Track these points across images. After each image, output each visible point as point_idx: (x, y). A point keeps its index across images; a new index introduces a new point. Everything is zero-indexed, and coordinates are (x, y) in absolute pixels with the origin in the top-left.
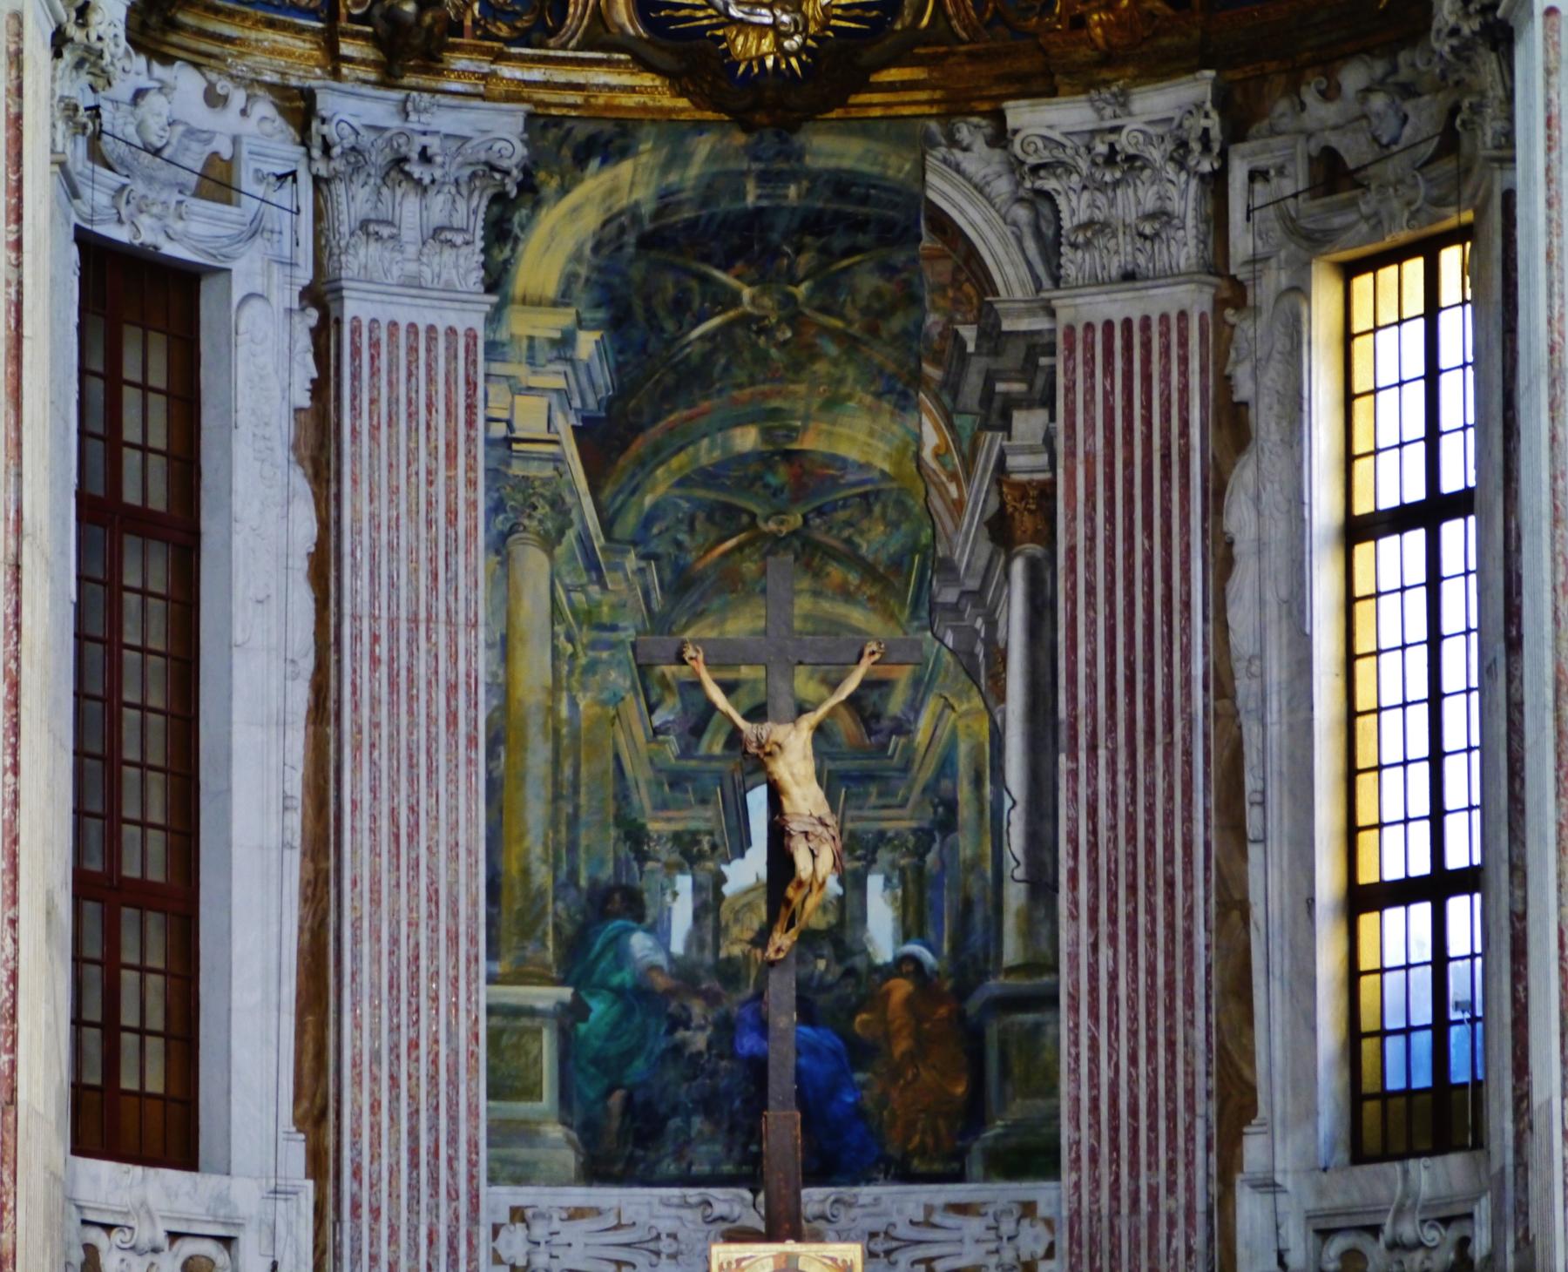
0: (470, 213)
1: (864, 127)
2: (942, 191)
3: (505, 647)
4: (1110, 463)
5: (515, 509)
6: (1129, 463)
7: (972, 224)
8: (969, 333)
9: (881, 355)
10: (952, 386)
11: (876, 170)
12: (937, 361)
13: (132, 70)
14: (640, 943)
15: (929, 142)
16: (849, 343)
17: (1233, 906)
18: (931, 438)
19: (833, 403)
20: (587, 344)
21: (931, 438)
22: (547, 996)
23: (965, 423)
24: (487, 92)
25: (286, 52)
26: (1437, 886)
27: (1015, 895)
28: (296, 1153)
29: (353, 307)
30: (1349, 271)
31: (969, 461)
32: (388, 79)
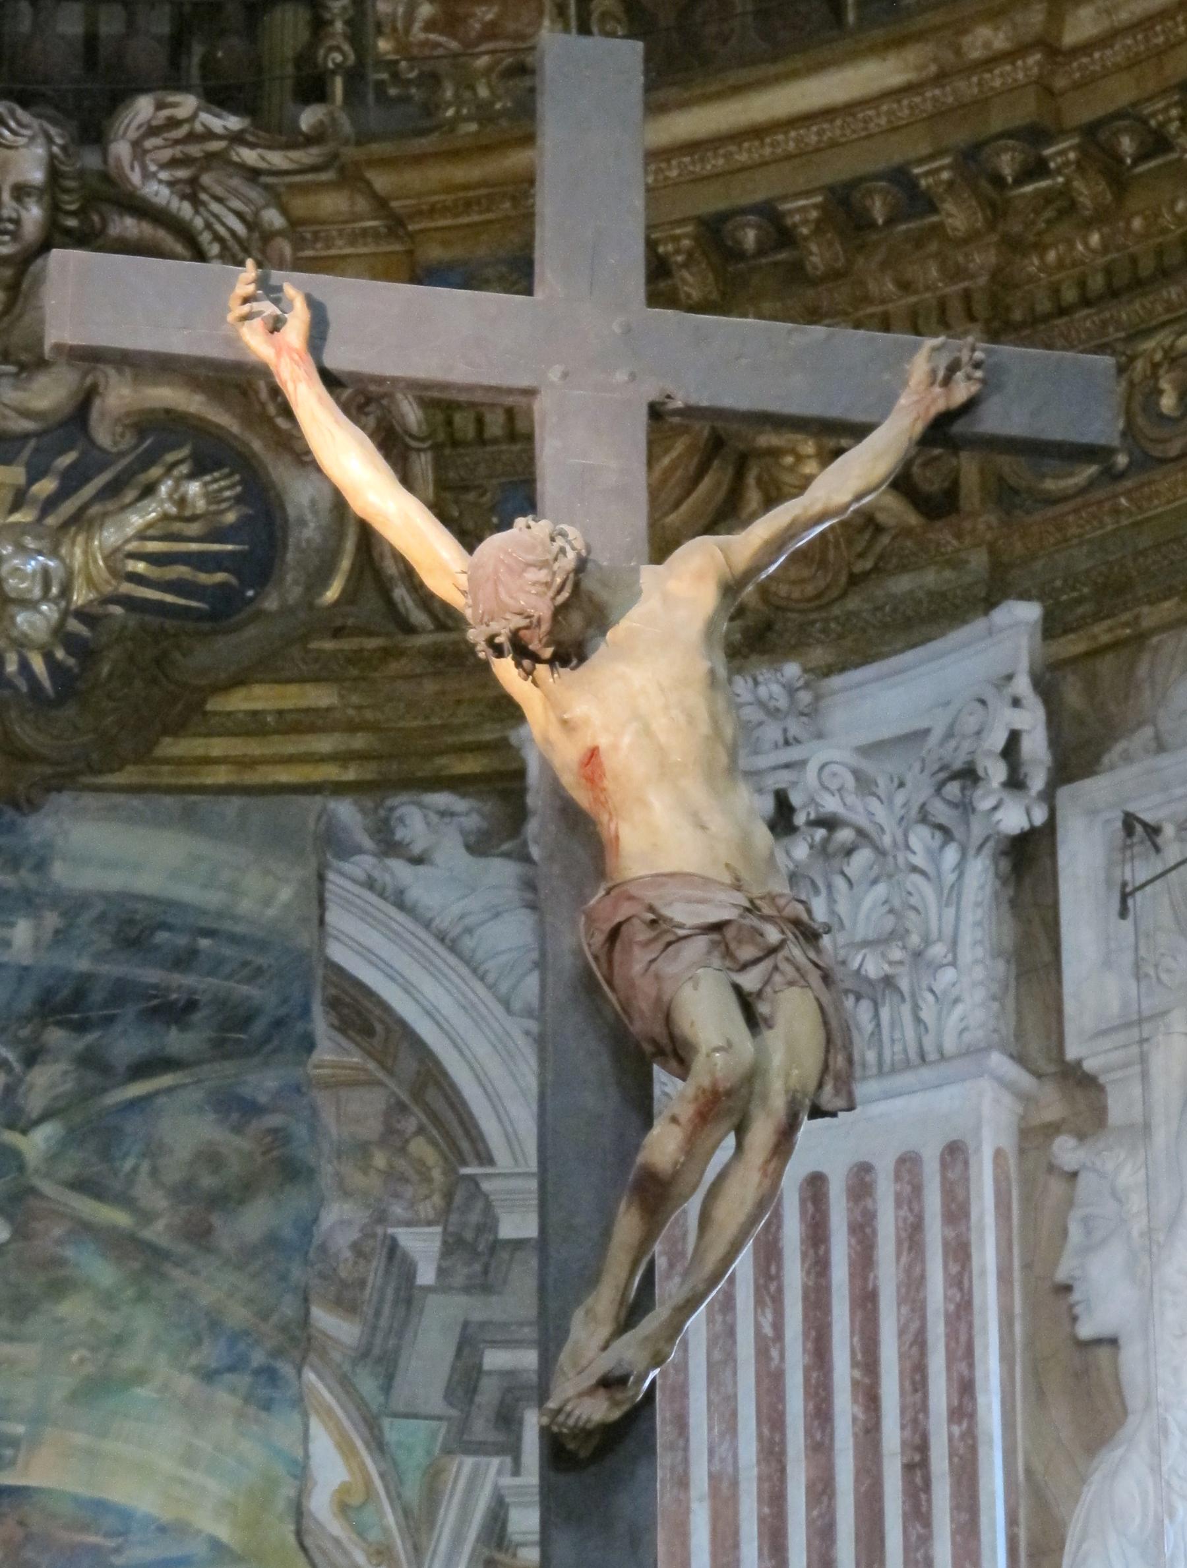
1: (186, 800)
4: (775, 1498)
6: (822, 1489)
7: (430, 1014)
8: (422, 1246)
9: (215, 1287)
10: (385, 1362)
11: (213, 899)
12: (346, 1304)
15: (333, 843)
16: (146, 1260)
18: (330, 1470)
19: (98, 1388)
21: (330, 1470)
23: (413, 1439)
31: (419, 1521)
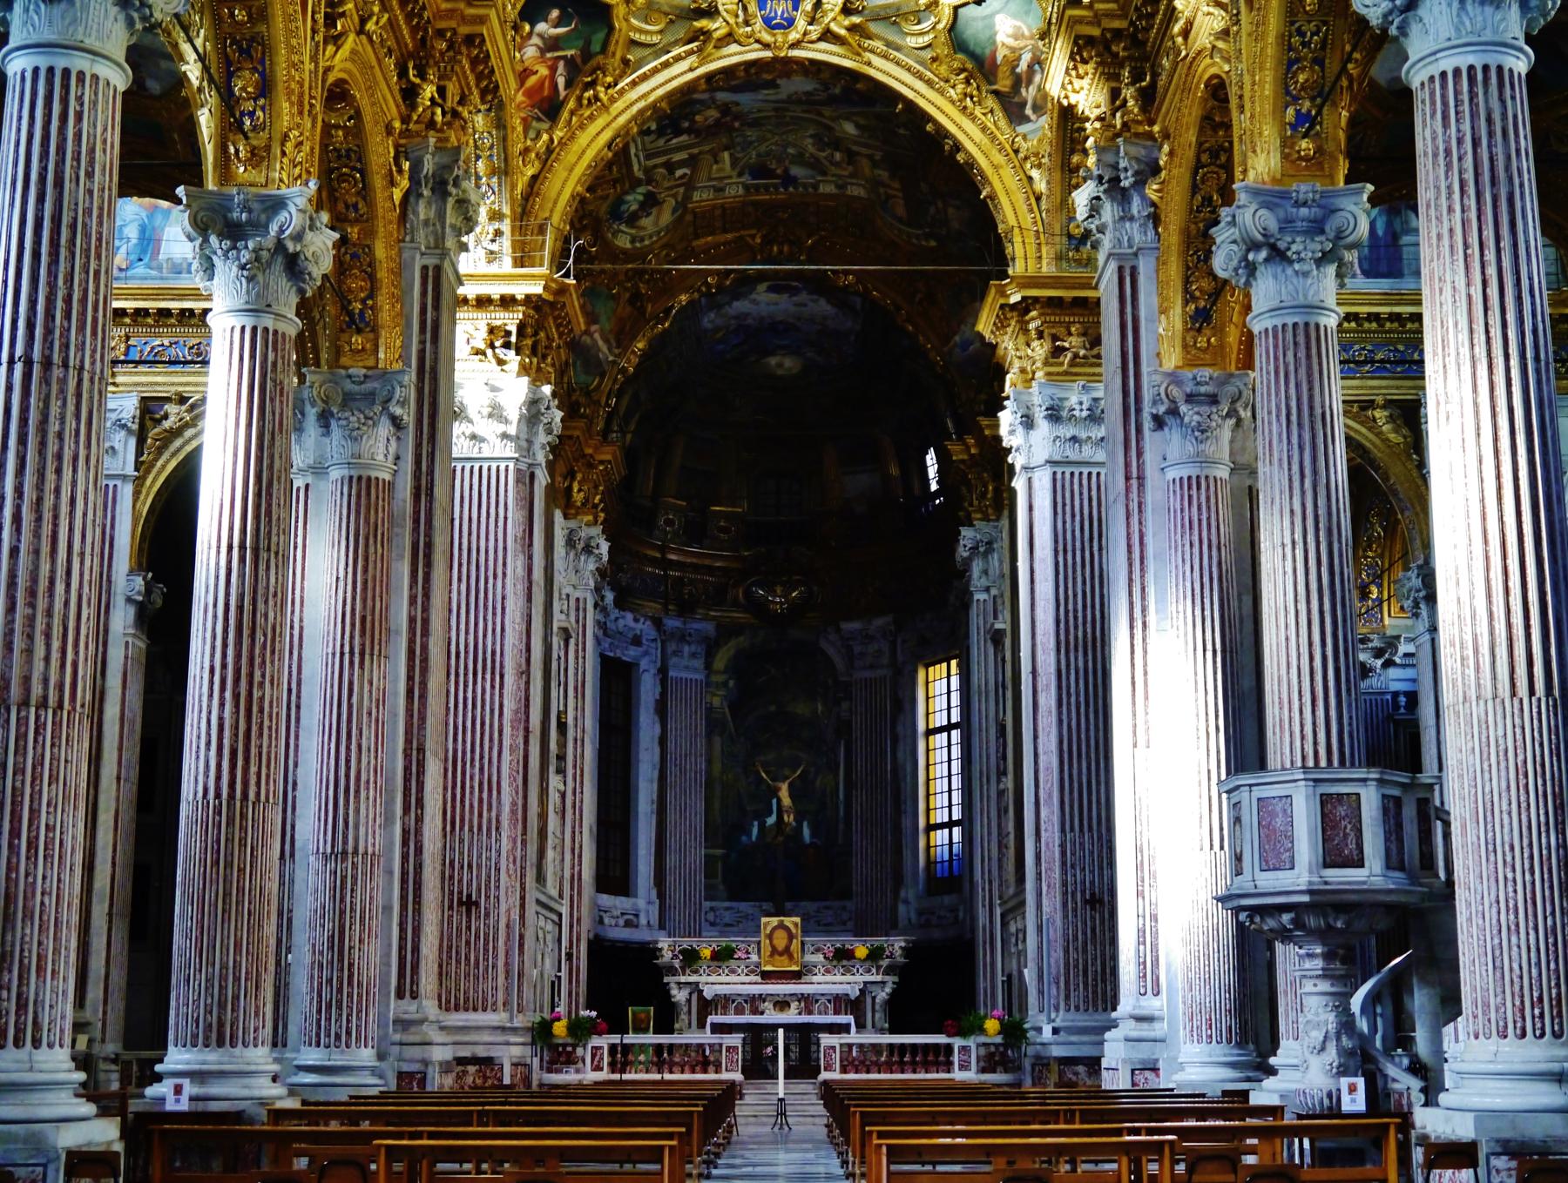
0: (700, 649)
2: (824, 645)
3: (709, 762)
5: (713, 725)
13: (615, 613)
14: (744, 838)
17: (897, 829)
20: (731, 683)
22: (719, 852)
24: (706, 618)
25: (653, 607)
26: (950, 824)
27: (841, 826)
28: (654, 893)
29: (671, 673)
30: (927, 667)
32: (679, 616)
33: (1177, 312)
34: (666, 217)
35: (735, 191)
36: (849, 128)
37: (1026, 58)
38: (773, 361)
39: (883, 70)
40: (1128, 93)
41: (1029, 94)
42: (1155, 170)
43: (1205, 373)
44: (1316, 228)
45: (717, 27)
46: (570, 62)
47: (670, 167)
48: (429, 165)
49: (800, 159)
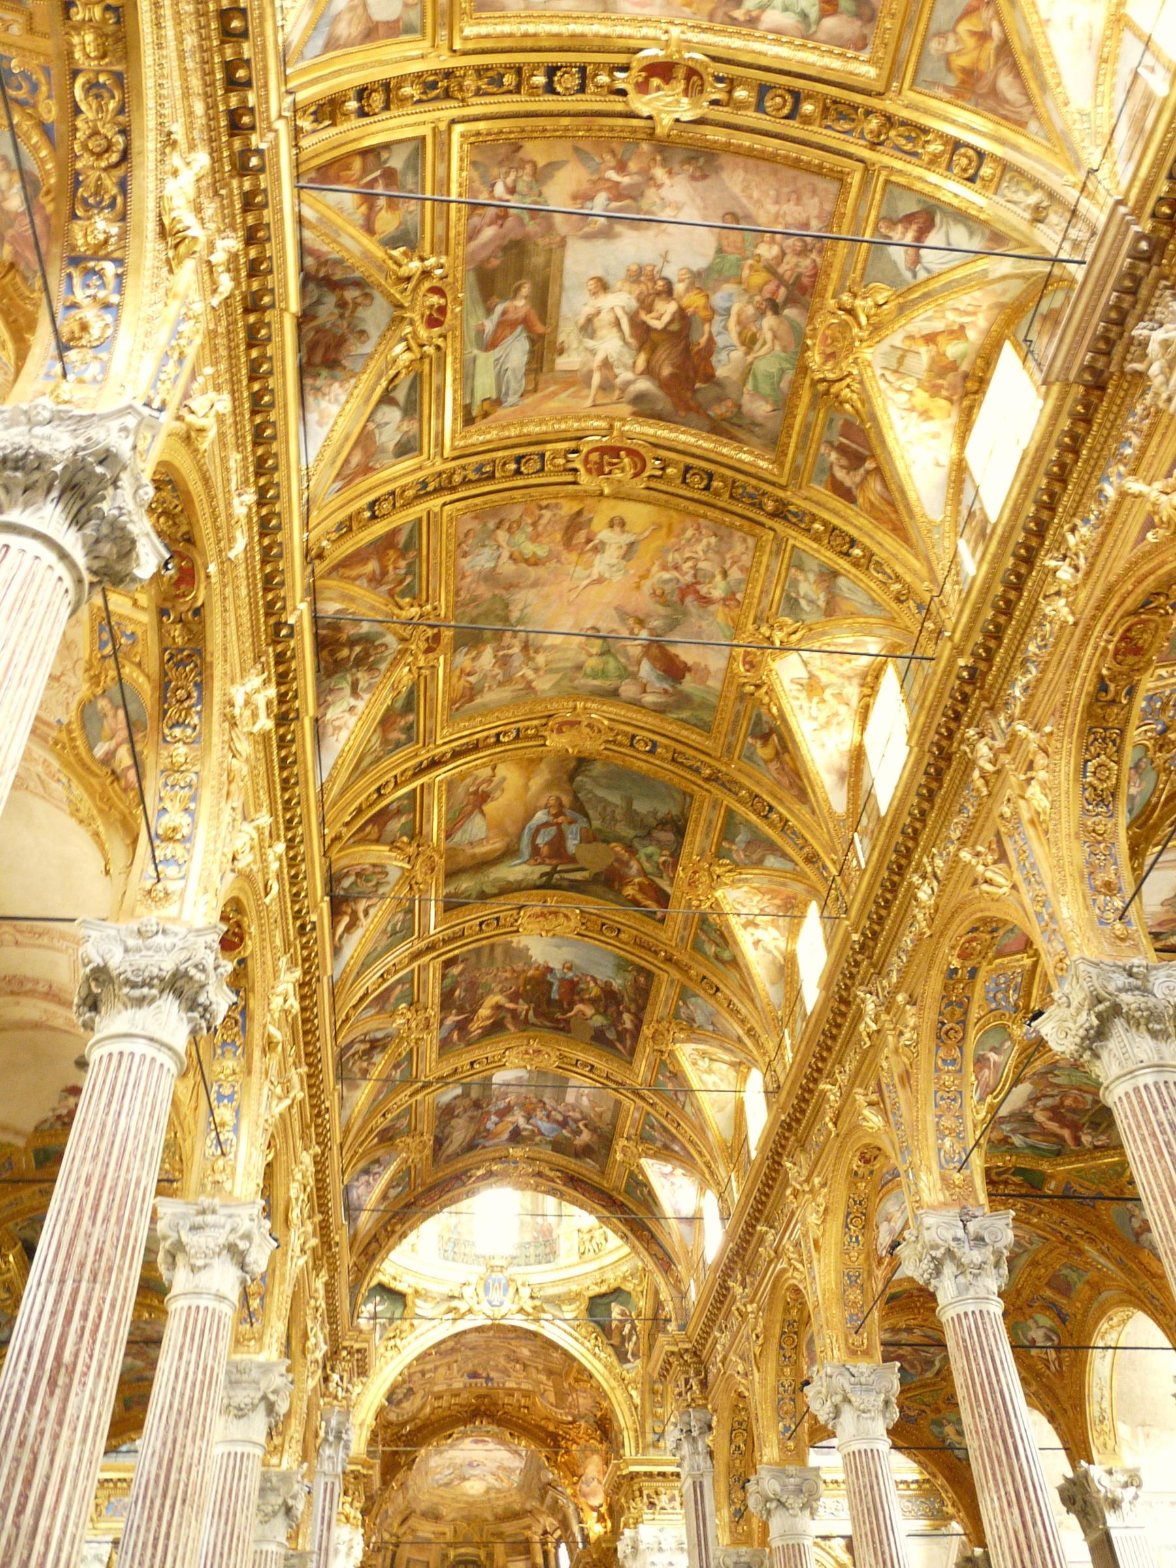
33: (725, 1513)
34: (417, 1401)
35: (458, 1384)
36: (526, 1352)
37: (628, 1326)
38: (467, 1484)
39: (551, 1331)
40: (693, 1382)
41: (630, 1346)
42: (710, 1428)
43: (743, 1549)
44: (799, 1491)
45: (463, 1306)
46: (383, 1326)
47: (423, 1373)
48: (333, 1423)
49: (496, 1368)
